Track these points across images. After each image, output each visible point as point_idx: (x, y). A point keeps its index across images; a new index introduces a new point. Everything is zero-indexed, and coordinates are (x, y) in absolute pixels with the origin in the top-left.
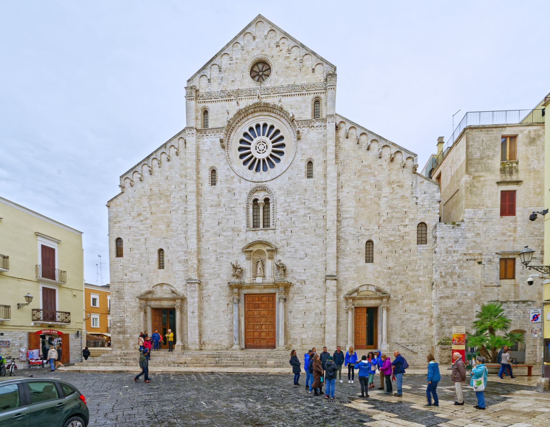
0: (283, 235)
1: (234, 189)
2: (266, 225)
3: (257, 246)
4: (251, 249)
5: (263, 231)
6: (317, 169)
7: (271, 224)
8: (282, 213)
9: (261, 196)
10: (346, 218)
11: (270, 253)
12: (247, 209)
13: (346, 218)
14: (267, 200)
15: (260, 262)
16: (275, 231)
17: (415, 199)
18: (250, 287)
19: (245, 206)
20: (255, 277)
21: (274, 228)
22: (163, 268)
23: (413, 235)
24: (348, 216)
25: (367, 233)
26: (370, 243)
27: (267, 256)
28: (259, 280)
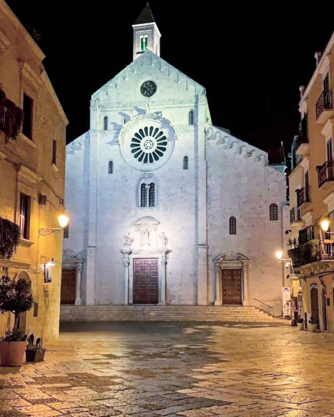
0: (164, 212)
1: (126, 177)
2: (152, 204)
3: (144, 220)
4: (139, 223)
5: (149, 209)
6: (191, 163)
7: (156, 203)
8: (164, 196)
9: (148, 182)
10: (214, 200)
11: (154, 226)
12: (137, 191)
13: (214, 200)
14: (152, 185)
15: (147, 233)
16: (159, 209)
17: (267, 186)
18: (136, 253)
19: (135, 189)
20: (142, 245)
21: (158, 207)
22: (68, 237)
23: (267, 215)
24: (215, 198)
25: (230, 211)
26: (233, 221)
27: (152, 229)
28: (145, 248)
